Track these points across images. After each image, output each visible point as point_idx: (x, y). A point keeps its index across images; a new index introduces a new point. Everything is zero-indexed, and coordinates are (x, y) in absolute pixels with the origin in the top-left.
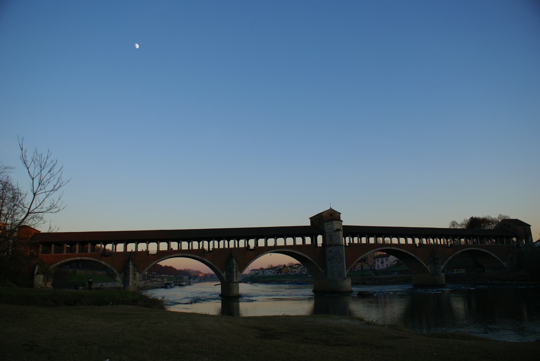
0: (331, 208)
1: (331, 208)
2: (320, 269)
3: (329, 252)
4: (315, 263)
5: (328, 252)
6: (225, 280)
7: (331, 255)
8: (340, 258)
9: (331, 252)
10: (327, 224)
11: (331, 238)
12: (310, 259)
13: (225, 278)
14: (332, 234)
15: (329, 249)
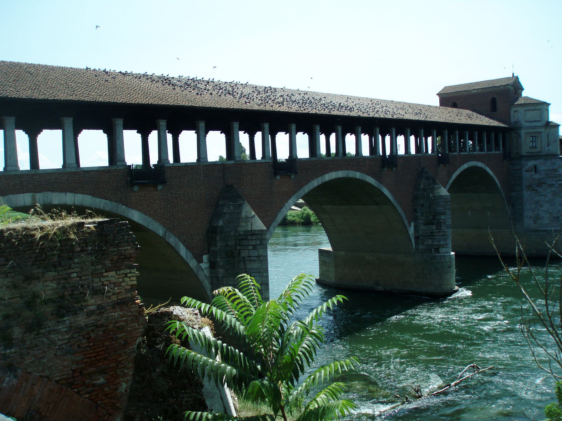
0: (513, 74)
1: (513, 74)
2: (507, 207)
3: (531, 171)
4: (503, 195)
5: (527, 171)
6: (414, 246)
7: (534, 176)
8: (559, 184)
9: (536, 172)
10: (525, 110)
11: (535, 141)
12: (499, 185)
13: (413, 240)
14: (540, 132)
15: (531, 163)
